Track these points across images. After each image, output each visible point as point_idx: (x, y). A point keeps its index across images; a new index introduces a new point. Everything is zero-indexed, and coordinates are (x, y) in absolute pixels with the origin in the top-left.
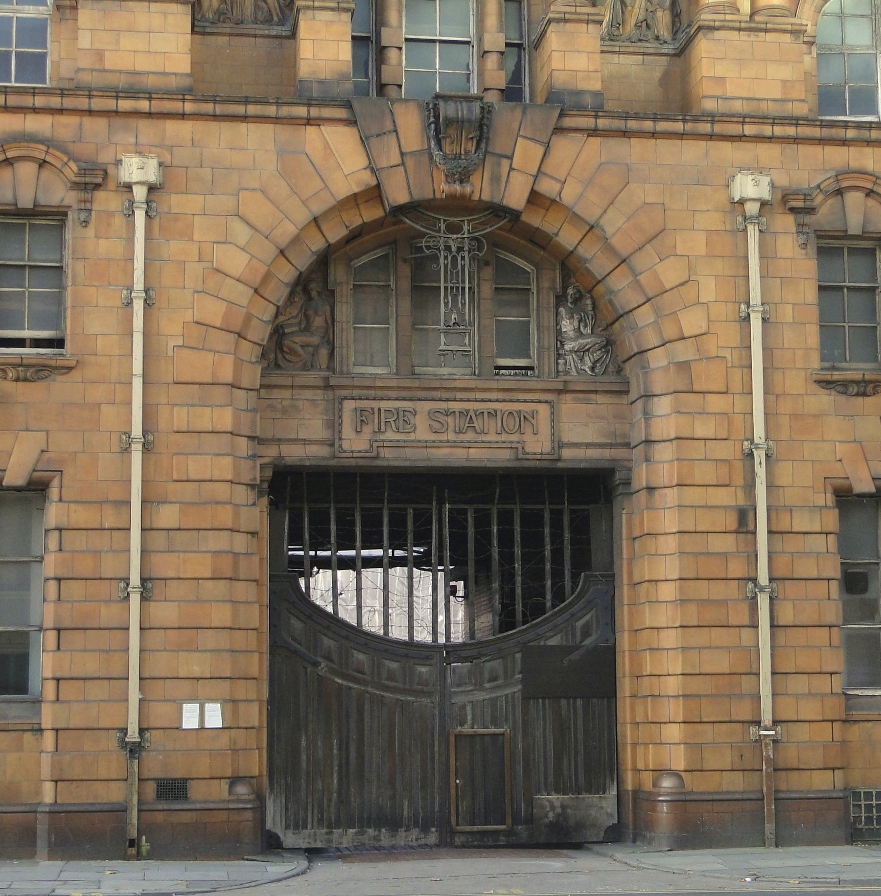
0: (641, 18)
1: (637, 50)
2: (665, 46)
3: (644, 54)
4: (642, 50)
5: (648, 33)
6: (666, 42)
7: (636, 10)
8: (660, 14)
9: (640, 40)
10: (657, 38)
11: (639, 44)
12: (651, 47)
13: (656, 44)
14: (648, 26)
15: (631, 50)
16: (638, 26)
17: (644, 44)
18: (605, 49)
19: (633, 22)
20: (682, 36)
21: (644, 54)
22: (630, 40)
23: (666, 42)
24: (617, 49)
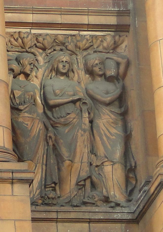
0: (84, 174)
1: (80, 216)
2: (118, 209)
3: (90, 221)
4: (87, 216)
5: (94, 193)
6: (118, 205)
7: (77, 165)
8: (108, 168)
9: (85, 203)
10: (106, 200)
11: (84, 208)
12: (100, 211)
13: (104, 208)
14: (93, 186)
15: (72, 216)
16: (80, 185)
17: (89, 208)
18: (38, 215)
19: (74, 181)
20: (137, 195)
21: (90, 221)
22: (69, 203)
23: (118, 205)
24: (54, 215)
